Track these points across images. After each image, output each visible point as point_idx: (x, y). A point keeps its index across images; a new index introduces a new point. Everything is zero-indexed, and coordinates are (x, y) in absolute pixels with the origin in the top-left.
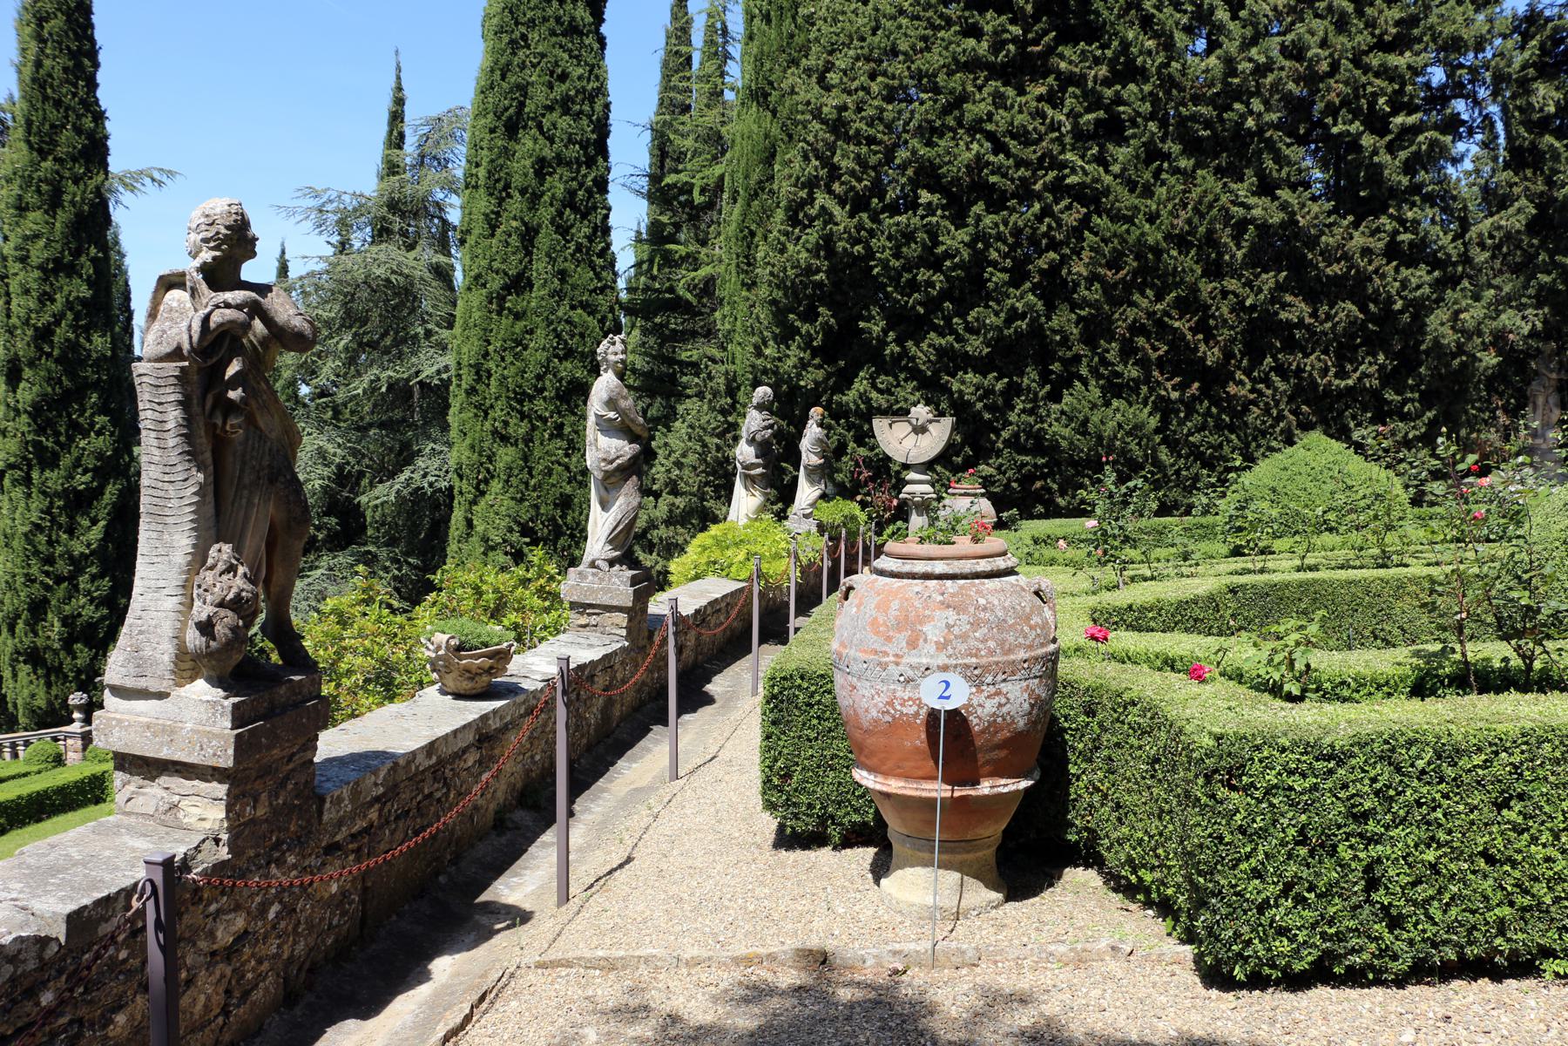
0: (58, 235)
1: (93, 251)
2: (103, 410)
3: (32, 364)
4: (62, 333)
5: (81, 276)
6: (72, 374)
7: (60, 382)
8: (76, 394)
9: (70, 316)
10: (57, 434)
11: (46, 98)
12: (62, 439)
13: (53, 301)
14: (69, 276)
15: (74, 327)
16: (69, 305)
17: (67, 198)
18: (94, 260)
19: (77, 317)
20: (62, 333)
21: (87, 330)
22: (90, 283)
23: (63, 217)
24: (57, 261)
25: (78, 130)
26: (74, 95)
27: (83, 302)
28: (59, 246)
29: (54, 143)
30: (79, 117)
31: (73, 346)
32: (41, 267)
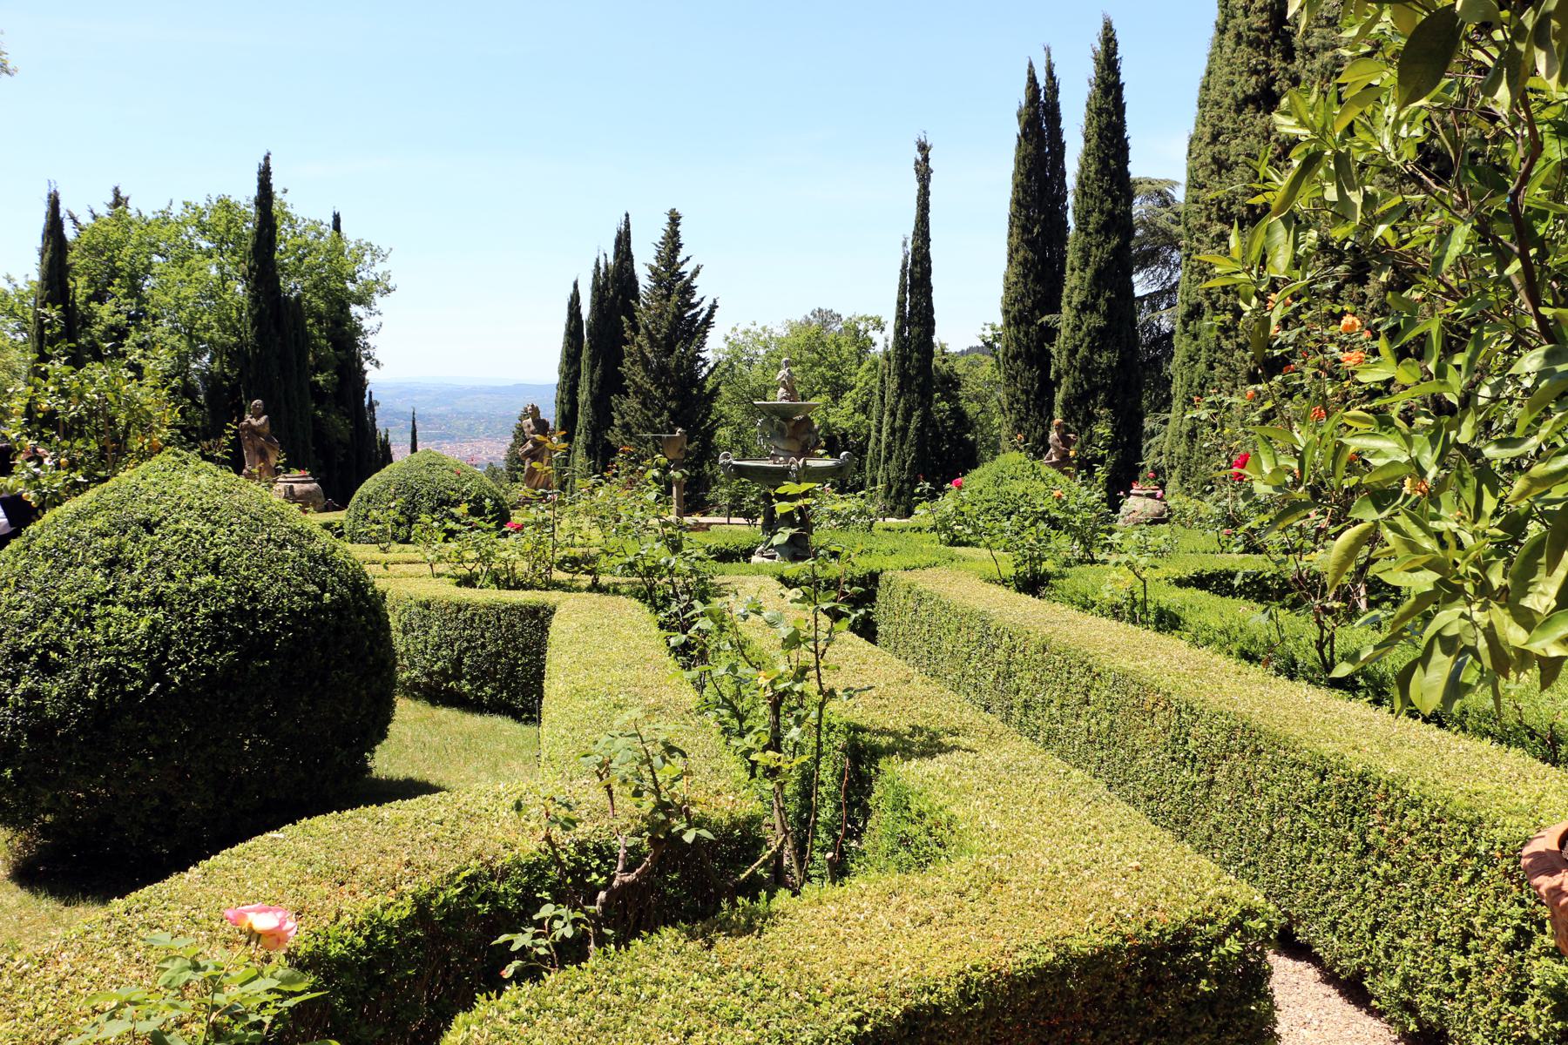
0: (1086, 285)
1: (1108, 294)
2: (1107, 404)
3: (1067, 373)
4: (1083, 352)
5: (1098, 312)
6: (1089, 380)
7: (1081, 386)
8: (1092, 393)
9: (1088, 340)
10: (1077, 420)
11: (1085, 194)
12: (1080, 424)
13: (1080, 329)
14: (1092, 313)
15: (1091, 349)
16: (1089, 333)
17: (1092, 259)
18: (1108, 300)
19: (1092, 342)
20: (1083, 352)
21: (1101, 348)
22: (1106, 316)
23: (1089, 272)
24: (1083, 303)
25: (1102, 212)
26: (1100, 187)
27: (1099, 330)
28: (1085, 293)
29: (1088, 223)
30: (1102, 202)
31: (1088, 361)
32: (1076, 308)
